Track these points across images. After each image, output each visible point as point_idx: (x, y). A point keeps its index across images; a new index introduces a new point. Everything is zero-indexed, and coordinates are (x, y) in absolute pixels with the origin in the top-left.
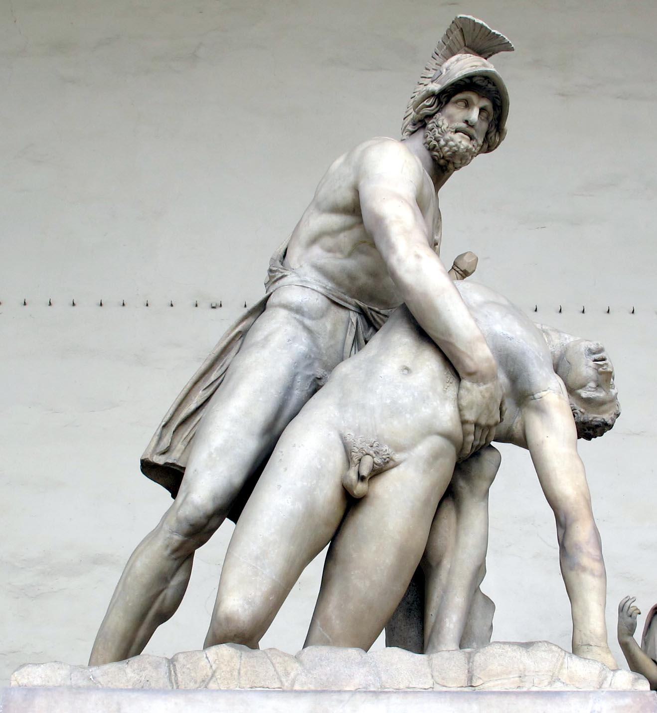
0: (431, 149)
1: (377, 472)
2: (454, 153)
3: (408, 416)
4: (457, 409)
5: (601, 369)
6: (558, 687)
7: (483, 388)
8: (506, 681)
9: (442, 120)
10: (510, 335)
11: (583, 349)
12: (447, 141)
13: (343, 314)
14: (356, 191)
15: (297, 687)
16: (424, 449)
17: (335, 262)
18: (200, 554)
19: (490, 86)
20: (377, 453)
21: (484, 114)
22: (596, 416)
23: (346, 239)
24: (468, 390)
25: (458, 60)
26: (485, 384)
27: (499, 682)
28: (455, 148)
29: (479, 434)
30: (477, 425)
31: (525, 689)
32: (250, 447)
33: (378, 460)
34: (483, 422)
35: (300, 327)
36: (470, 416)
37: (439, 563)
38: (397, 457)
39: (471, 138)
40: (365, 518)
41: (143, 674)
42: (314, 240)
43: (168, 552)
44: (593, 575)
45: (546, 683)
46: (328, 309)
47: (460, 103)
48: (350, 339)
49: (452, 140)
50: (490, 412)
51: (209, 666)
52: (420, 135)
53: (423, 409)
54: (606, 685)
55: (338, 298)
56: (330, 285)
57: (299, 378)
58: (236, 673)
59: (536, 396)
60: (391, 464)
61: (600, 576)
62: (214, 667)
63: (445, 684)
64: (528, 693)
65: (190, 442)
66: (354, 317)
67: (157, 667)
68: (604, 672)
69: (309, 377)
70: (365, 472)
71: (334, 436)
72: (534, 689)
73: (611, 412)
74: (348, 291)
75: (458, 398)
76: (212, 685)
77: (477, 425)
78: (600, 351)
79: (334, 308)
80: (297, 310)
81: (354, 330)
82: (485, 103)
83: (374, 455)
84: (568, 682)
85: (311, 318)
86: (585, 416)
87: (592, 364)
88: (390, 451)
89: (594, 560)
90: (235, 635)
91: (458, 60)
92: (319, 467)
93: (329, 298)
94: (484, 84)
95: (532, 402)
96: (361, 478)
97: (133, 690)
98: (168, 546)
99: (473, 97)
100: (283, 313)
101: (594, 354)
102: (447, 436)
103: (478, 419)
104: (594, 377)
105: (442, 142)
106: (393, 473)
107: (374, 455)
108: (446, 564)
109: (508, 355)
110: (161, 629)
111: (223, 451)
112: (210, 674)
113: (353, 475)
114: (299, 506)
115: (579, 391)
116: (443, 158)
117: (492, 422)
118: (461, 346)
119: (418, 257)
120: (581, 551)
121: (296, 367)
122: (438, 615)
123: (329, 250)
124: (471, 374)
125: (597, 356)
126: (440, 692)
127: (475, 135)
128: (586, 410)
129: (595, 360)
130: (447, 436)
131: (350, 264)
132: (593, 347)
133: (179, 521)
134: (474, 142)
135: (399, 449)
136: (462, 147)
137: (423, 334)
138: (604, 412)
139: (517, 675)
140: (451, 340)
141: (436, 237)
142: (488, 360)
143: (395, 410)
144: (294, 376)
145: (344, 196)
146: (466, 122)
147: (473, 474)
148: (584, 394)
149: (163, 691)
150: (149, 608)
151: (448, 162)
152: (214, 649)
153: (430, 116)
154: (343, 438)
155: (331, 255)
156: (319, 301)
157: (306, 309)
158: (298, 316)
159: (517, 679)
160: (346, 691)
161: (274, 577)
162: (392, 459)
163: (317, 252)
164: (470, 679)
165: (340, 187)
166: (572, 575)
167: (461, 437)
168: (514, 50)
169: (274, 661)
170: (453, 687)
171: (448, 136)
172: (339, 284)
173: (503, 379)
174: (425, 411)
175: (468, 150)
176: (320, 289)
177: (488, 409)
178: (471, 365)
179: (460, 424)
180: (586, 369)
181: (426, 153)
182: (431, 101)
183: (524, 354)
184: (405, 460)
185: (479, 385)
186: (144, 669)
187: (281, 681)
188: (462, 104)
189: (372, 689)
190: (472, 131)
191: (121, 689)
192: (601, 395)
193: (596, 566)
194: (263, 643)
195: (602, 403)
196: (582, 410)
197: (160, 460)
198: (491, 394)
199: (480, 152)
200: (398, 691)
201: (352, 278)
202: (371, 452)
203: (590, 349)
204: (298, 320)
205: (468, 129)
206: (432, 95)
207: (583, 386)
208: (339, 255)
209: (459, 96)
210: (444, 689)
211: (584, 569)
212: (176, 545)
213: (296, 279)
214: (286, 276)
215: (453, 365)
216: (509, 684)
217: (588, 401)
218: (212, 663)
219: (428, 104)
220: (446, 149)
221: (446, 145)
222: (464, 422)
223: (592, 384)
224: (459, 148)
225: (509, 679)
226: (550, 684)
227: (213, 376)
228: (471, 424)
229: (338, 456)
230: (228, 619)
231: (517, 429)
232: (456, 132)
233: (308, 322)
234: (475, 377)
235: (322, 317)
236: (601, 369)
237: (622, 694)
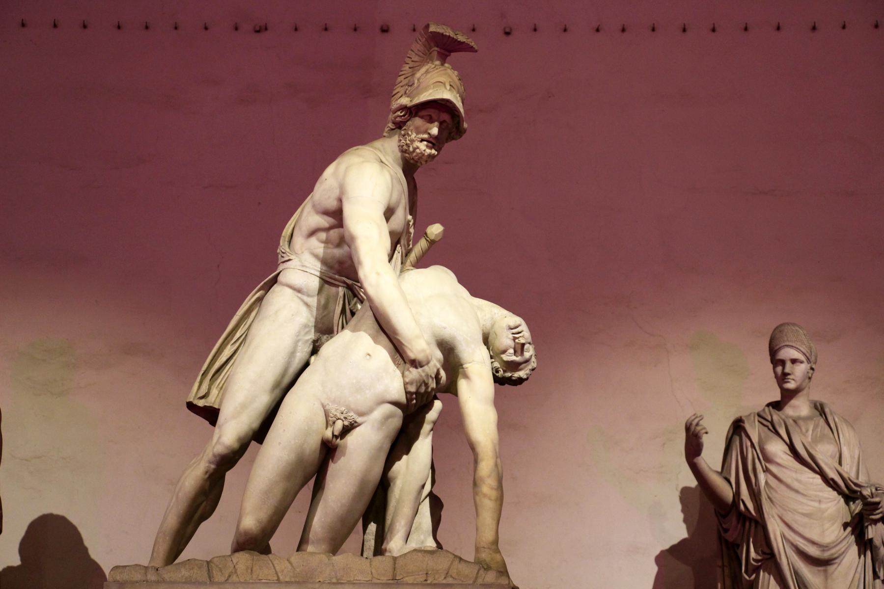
0: (403, 151)
1: (347, 430)
6: (450, 580)
7: (420, 370)
10: (444, 325)
11: (505, 325)
12: (415, 149)
13: (333, 289)
14: (340, 200)
18: (229, 476)
20: (345, 418)
25: (427, 72)
31: (429, 582)
32: (263, 401)
33: (346, 423)
35: (301, 303)
36: (412, 389)
38: (359, 420)
42: (313, 233)
43: (207, 476)
44: (490, 499)
48: (339, 309)
49: (418, 148)
50: (426, 385)
52: (396, 138)
54: (480, 581)
55: (330, 278)
57: (300, 344)
59: (464, 366)
64: (430, 584)
65: (223, 389)
66: (341, 291)
69: (308, 340)
70: (336, 433)
71: (318, 406)
72: (435, 582)
76: (234, 578)
78: (516, 327)
79: (326, 286)
81: (341, 302)
85: (309, 296)
89: (492, 489)
91: (427, 72)
97: (185, 583)
98: (206, 472)
100: (289, 291)
102: (396, 404)
105: (411, 149)
106: (358, 429)
110: (204, 525)
111: (244, 406)
114: (293, 457)
119: (378, 274)
121: (298, 336)
122: (392, 520)
126: (376, 584)
130: (396, 404)
131: (338, 252)
132: (512, 324)
133: (214, 455)
135: (361, 414)
142: (423, 351)
143: (359, 389)
144: (296, 343)
145: (332, 204)
148: (505, 357)
149: (205, 583)
150: (195, 512)
152: (237, 554)
153: (404, 123)
154: (323, 406)
158: (299, 295)
165: (329, 197)
166: (477, 498)
168: (476, 51)
170: (384, 579)
171: (417, 144)
173: (439, 355)
181: (399, 154)
183: (454, 338)
186: (193, 569)
189: (334, 580)
191: (179, 583)
192: (518, 359)
194: (272, 542)
197: (201, 403)
199: (447, 141)
200: (350, 583)
201: (341, 262)
204: (300, 298)
205: (431, 140)
206: (403, 108)
207: (504, 352)
208: (330, 246)
210: (379, 581)
212: (211, 471)
213: (299, 263)
214: (289, 260)
221: (414, 151)
222: (407, 393)
223: (512, 351)
227: (238, 335)
229: (321, 419)
230: (246, 533)
232: (422, 140)
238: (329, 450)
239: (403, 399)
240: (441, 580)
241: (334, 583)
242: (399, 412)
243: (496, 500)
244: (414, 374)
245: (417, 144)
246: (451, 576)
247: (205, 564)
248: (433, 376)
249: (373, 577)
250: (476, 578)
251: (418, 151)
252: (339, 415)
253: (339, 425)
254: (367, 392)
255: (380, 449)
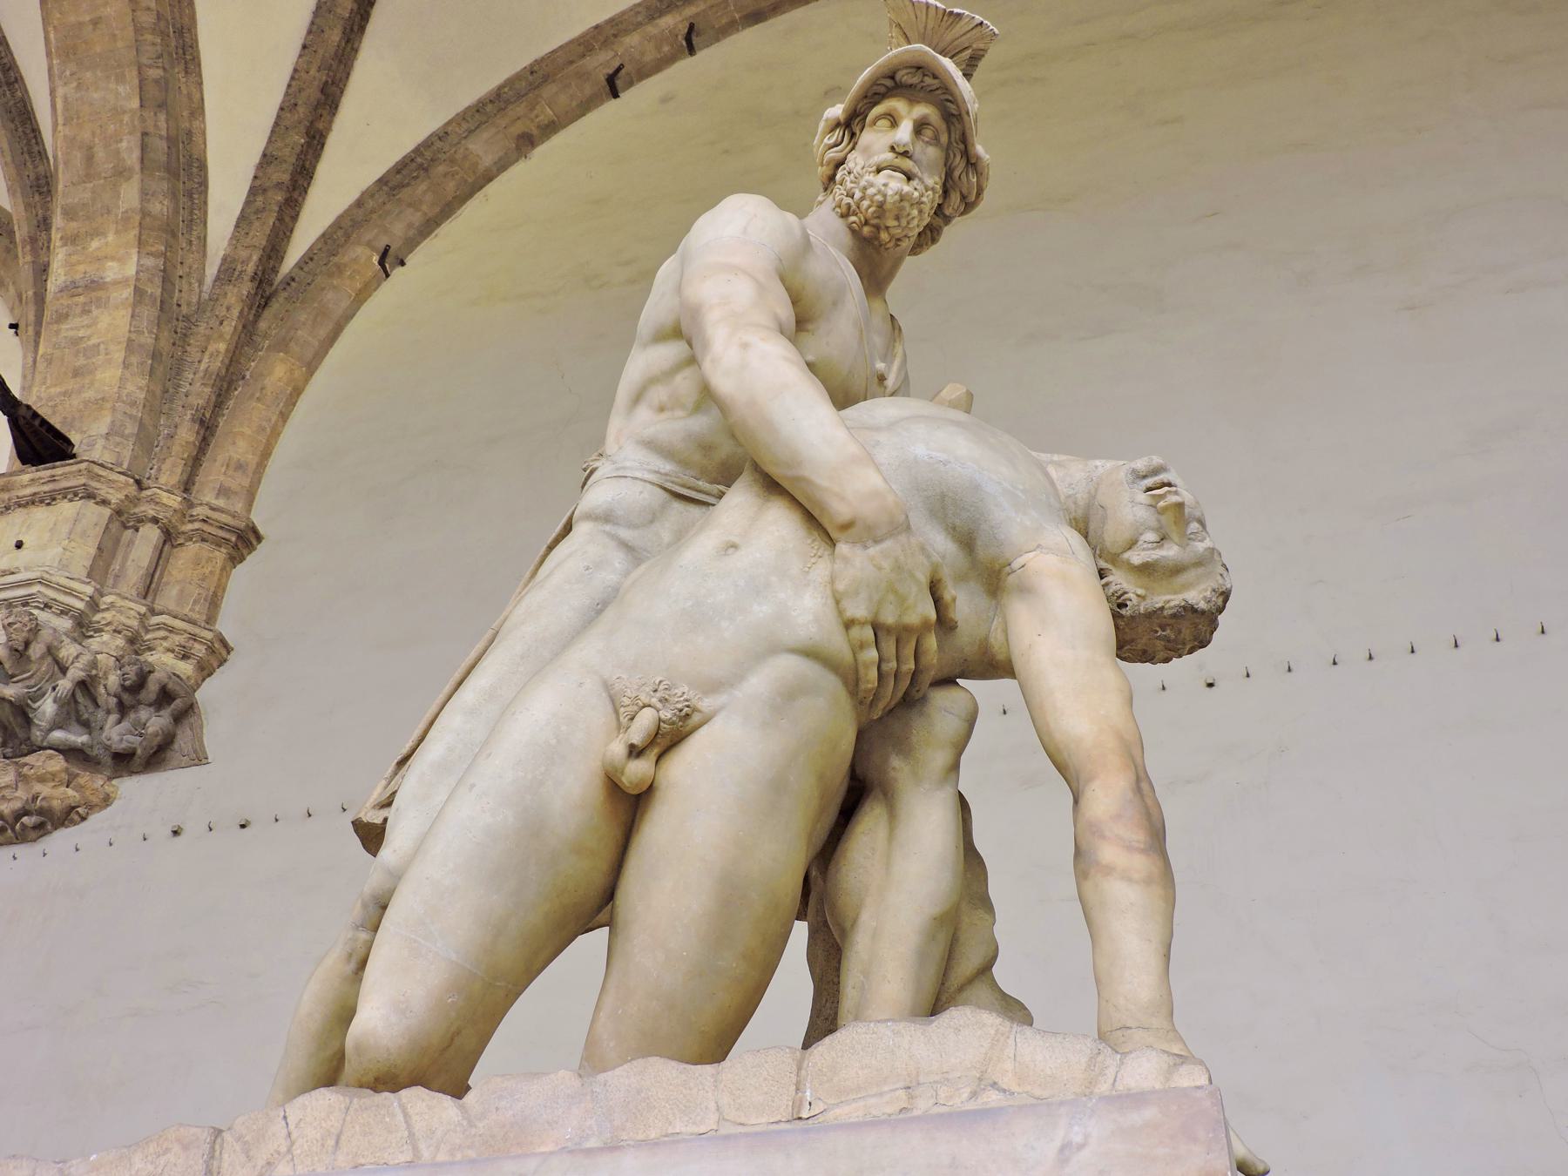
1: (667, 739)
2: (881, 206)
3: (724, 624)
4: (830, 601)
5: (1162, 504)
6: (992, 1098)
7: (874, 550)
8: (873, 1101)
9: (855, 161)
10: (943, 456)
15: (441, 1157)
16: (760, 682)
17: (677, 427)
19: (928, 80)
20: (664, 700)
21: (928, 133)
22: (1168, 597)
23: (684, 383)
24: (846, 560)
26: (877, 541)
27: (861, 1103)
28: (879, 198)
29: (889, 647)
30: (877, 628)
31: (916, 1113)
33: (666, 714)
34: (889, 617)
37: (855, 921)
38: (706, 704)
39: (909, 178)
40: (657, 829)
41: (162, 1160)
42: (637, 398)
44: (1130, 880)
45: (965, 1096)
46: (664, 507)
47: (880, 123)
49: (872, 185)
50: (902, 600)
51: (285, 1132)
53: (756, 607)
54: (1104, 1088)
55: (683, 486)
56: (667, 467)
58: (331, 1142)
59: (1015, 565)
60: (696, 718)
61: (1148, 881)
62: (294, 1136)
63: (743, 1120)
67: (186, 1148)
68: (1100, 1058)
73: (1203, 586)
74: (703, 473)
75: (832, 581)
77: (877, 628)
78: (1156, 471)
79: (678, 506)
80: (605, 517)
82: (922, 110)
83: (659, 705)
84: (1015, 1088)
85: (632, 526)
86: (1148, 601)
87: (1143, 498)
88: (690, 694)
89: (1129, 848)
90: (377, 1079)
92: (553, 742)
93: (665, 489)
94: (915, 80)
95: (1011, 578)
96: (635, 752)
98: (350, 955)
99: (897, 104)
101: (1145, 477)
102: (810, 653)
103: (877, 614)
104: (1154, 524)
105: (858, 195)
107: (659, 705)
108: (866, 921)
109: (943, 496)
112: (283, 1149)
113: (618, 749)
115: (1126, 555)
116: (866, 223)
117: (913, 619)
118: (822, 481)
120: (1103, 837)
123: (662, 409)
124: (846, 526)
125: (1149, 482)
126: (727, 1137)
127: (916, 170)
128: (1147, 589)
129: (1149, 489)
130: (810, 653)
131: (700, 424)
134: (915, 183)
135: (714, 686)
136: (890, 192)
137: (772, 486)
138: (1186, 587)
139: (901, 1084)
140: (806, 473)
141: (880, 366)
146: (893, 149)
147: (914, 739)
148: (1136, 557)
151: (877, 228)
154: (607, 686)
155: (664, 416)
156: (645, 495)
157: (620, 513)
158: (608, 528)
159: (902, 1093)
160: (535, 1155)
161: (454, 957)
162: (695, 710)
163: (644, 413)
164: (797, 1104)
167: (847, 656)
169: (410, 1111)
170: (759, 1121)
172: (683, 463)
173: (942, 544)
174: (761, 610)
175: (903, 198)
176: (647, 476)
177: (896, 592)
178: (840, 510)
179: (841, 628)
180: (1129, 510)
181: (839, 225)
182: (838, 133)
183: (977, 488)
184: (722, 708)
185: (866, 547)
186: (167, 1151)
187: (415, 1149)
188: (883, 123)
189: (592, 1143)
190: (907, 164)
192: (1171, 552)
193: (1140, 864)
195: (1176, 570)
196: (1140, 592)
198: (896, 561)
201: (706, 448)
202: (654, 701)
203: (1134, 471)
204: (609, 534)
207: (1132, 544)
208: (679, 413)
209: (877, 110)
210: (741, 1129)
211: (1108, 870)
215: (816, 521)
216: (884, 1106)
217: (1146, 569)
218: (292, 1127)
219: (832, 141)
220: (865, 203)
221: (863, 198)
222: (848, 624)
223: (1151, 536)
224: (885, 196)
225: (881, 1094)
226: (974, 1095)
228: (863, 624)
229: (599, 714)
231: (996, 640)
232: (879, 171)
233: (625, 533)
234: (853, 531)
235: (652, 522)
236: (1162, 504)
237: (1136, 1099)
238: (629, 805)
239: (838, 644)
240: (960, 1100)
241: (589, 1152)
242: (831, 682)
243: (1148, 881)
244: (857, 563)
245: (871, 177)
246: (994, 1085)
247: (205, 1136)
248: (924, 579)
249: (722, 1119)
250: (1092, 1083)
251: (871, 191)
252: (644, 699)
253: (646, 720)
254: (724, 624)
255: (777, 786)
